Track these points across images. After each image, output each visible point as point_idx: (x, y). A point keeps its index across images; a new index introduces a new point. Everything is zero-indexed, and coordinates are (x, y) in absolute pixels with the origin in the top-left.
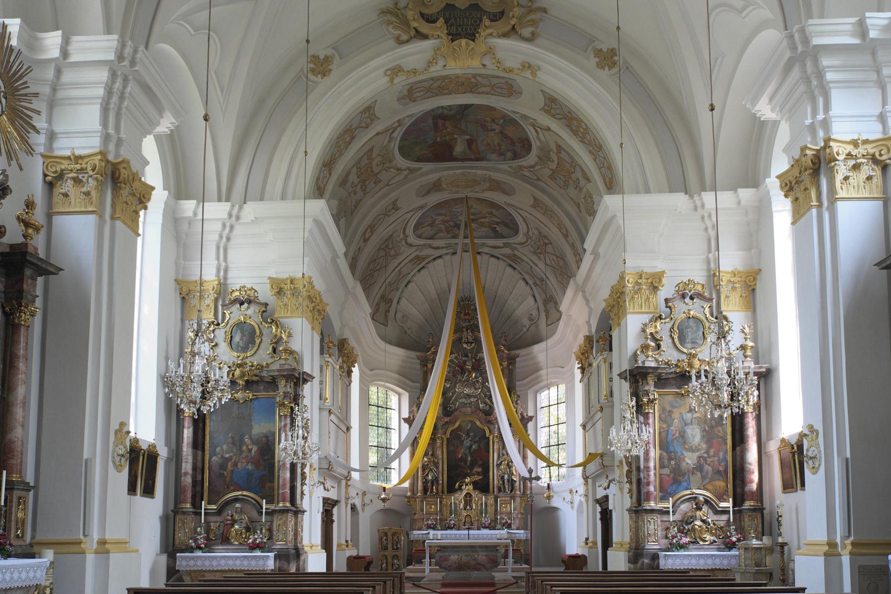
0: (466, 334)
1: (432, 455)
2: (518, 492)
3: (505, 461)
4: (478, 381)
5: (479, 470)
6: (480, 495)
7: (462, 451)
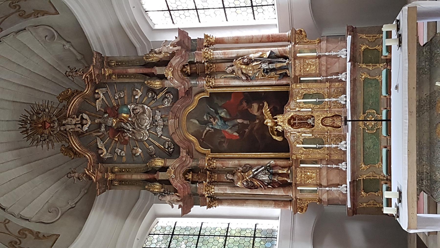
0: (70, 127)
1: (233, 174)
2: (287, 48)
3: (241, 69)
4: (134, 109)
5: (255, 106)
6: (292, 104)
7: (230, 131)
